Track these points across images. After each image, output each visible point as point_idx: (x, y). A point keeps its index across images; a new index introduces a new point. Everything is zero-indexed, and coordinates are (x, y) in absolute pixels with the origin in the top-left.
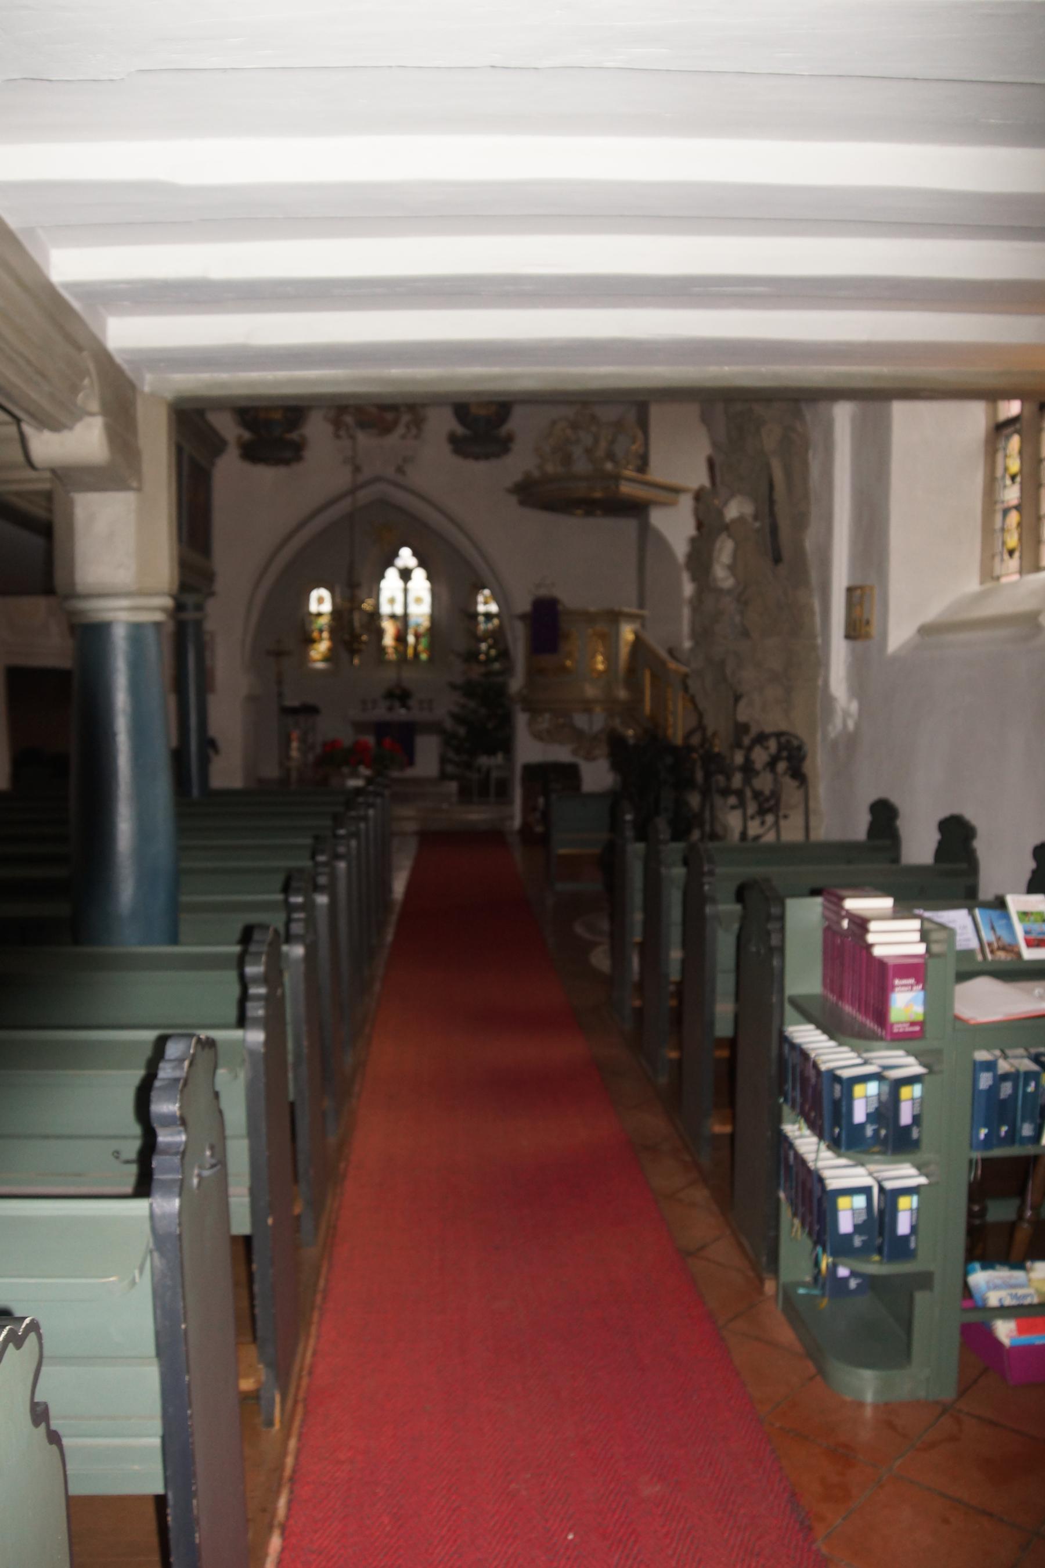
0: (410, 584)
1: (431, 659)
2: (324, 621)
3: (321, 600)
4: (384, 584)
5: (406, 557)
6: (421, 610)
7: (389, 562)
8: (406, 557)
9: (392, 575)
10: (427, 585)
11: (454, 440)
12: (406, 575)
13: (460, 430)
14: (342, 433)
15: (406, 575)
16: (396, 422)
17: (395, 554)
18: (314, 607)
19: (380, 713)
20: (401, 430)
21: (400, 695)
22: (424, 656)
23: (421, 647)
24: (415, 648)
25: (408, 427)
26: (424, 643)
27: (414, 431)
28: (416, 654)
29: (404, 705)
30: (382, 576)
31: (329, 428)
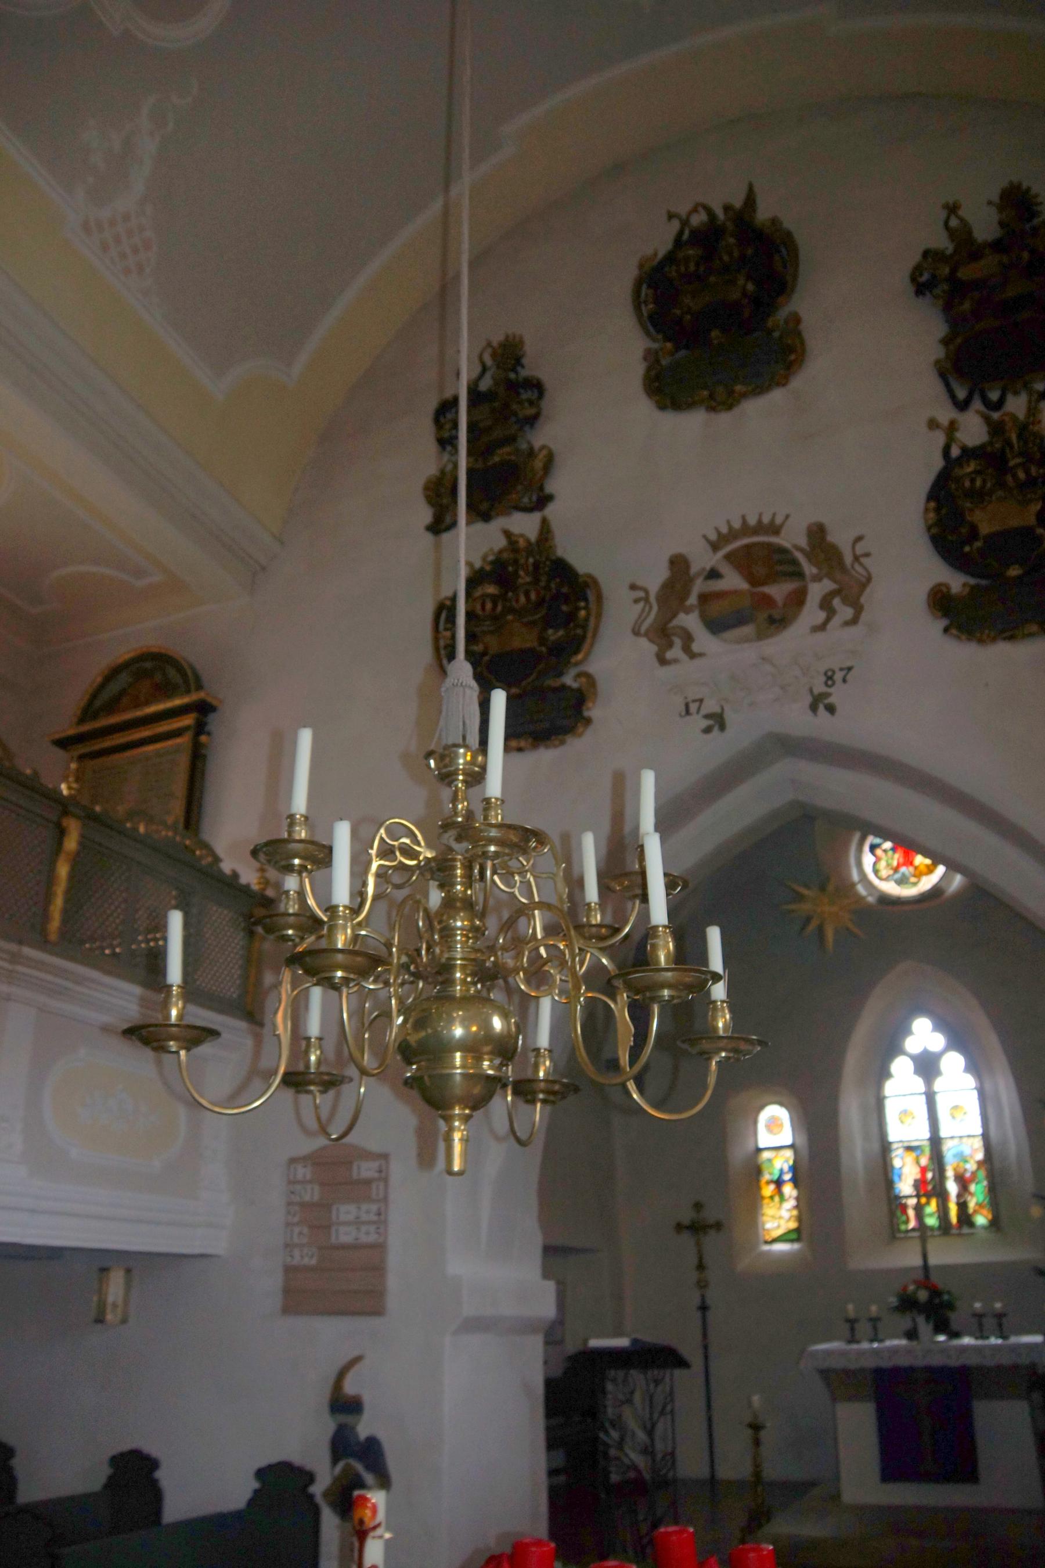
0: (938, 1085)
1: (995, 1223)
2: (781, 1163)
3: (773, 1125)
4: (890, 1088)
5: (923, 1035)
6: (965, 1135)
7: (892, 1047)
8: (923, 1035)
9: (901, 1067)
10: (970, 1081)
11: (941, 601)
12: (927, 1066)
13: (957, 582)
14: (676, 652)
15: (927, 1066)
16: (798, 599)
17: (903, 1030)
18: (764, 1139)
19: (893, 1346)
20: (811, 614)
21: (929, 1302)
22: (981, 1220)
23: (972, 1204)
24: (962, 1206)
25: (826, 604)
26: (978, 1192)
27: (846, 612)
28: (965, 1218)
29: (942, 1326)
30: (884, 1074)
31: (648, 648)
